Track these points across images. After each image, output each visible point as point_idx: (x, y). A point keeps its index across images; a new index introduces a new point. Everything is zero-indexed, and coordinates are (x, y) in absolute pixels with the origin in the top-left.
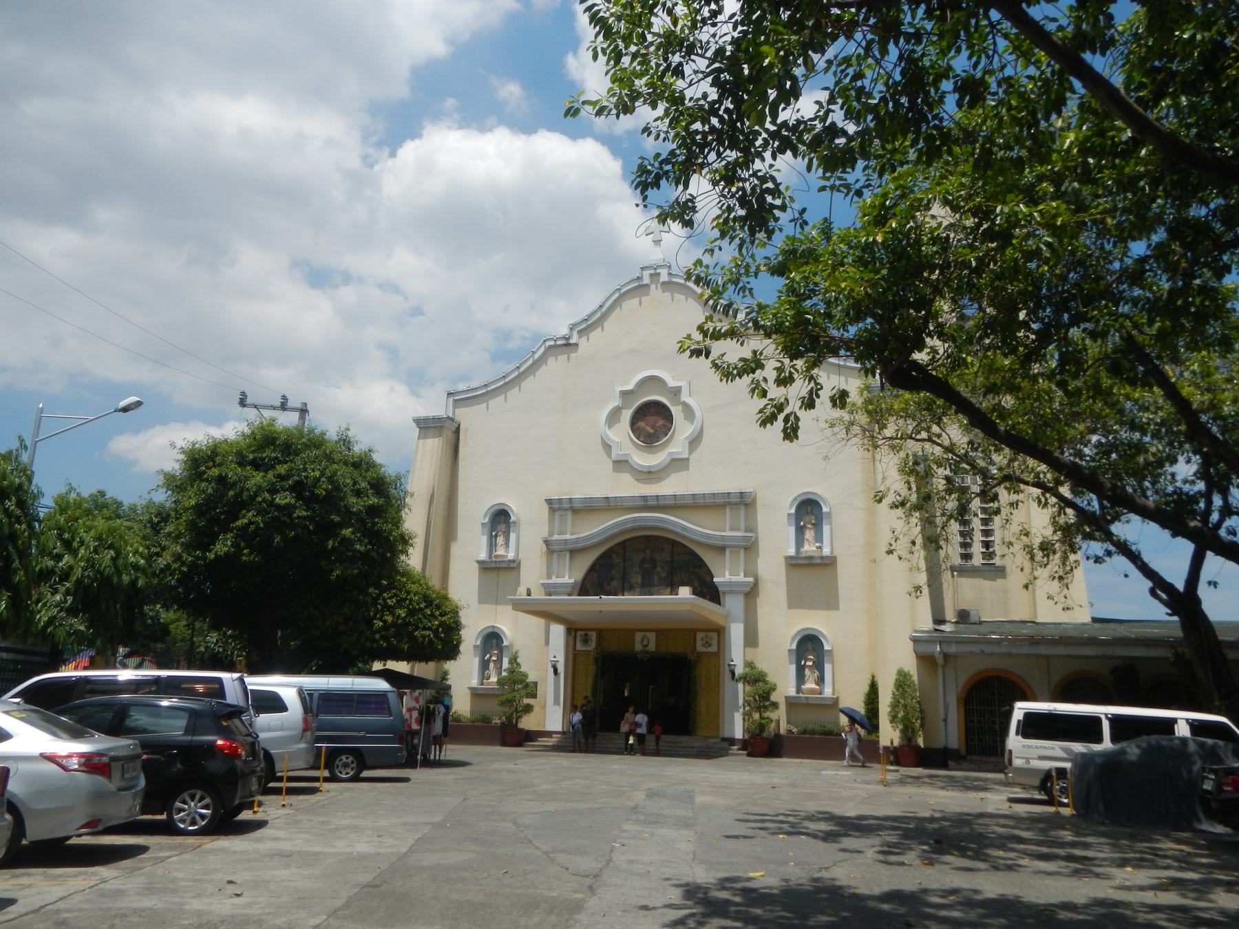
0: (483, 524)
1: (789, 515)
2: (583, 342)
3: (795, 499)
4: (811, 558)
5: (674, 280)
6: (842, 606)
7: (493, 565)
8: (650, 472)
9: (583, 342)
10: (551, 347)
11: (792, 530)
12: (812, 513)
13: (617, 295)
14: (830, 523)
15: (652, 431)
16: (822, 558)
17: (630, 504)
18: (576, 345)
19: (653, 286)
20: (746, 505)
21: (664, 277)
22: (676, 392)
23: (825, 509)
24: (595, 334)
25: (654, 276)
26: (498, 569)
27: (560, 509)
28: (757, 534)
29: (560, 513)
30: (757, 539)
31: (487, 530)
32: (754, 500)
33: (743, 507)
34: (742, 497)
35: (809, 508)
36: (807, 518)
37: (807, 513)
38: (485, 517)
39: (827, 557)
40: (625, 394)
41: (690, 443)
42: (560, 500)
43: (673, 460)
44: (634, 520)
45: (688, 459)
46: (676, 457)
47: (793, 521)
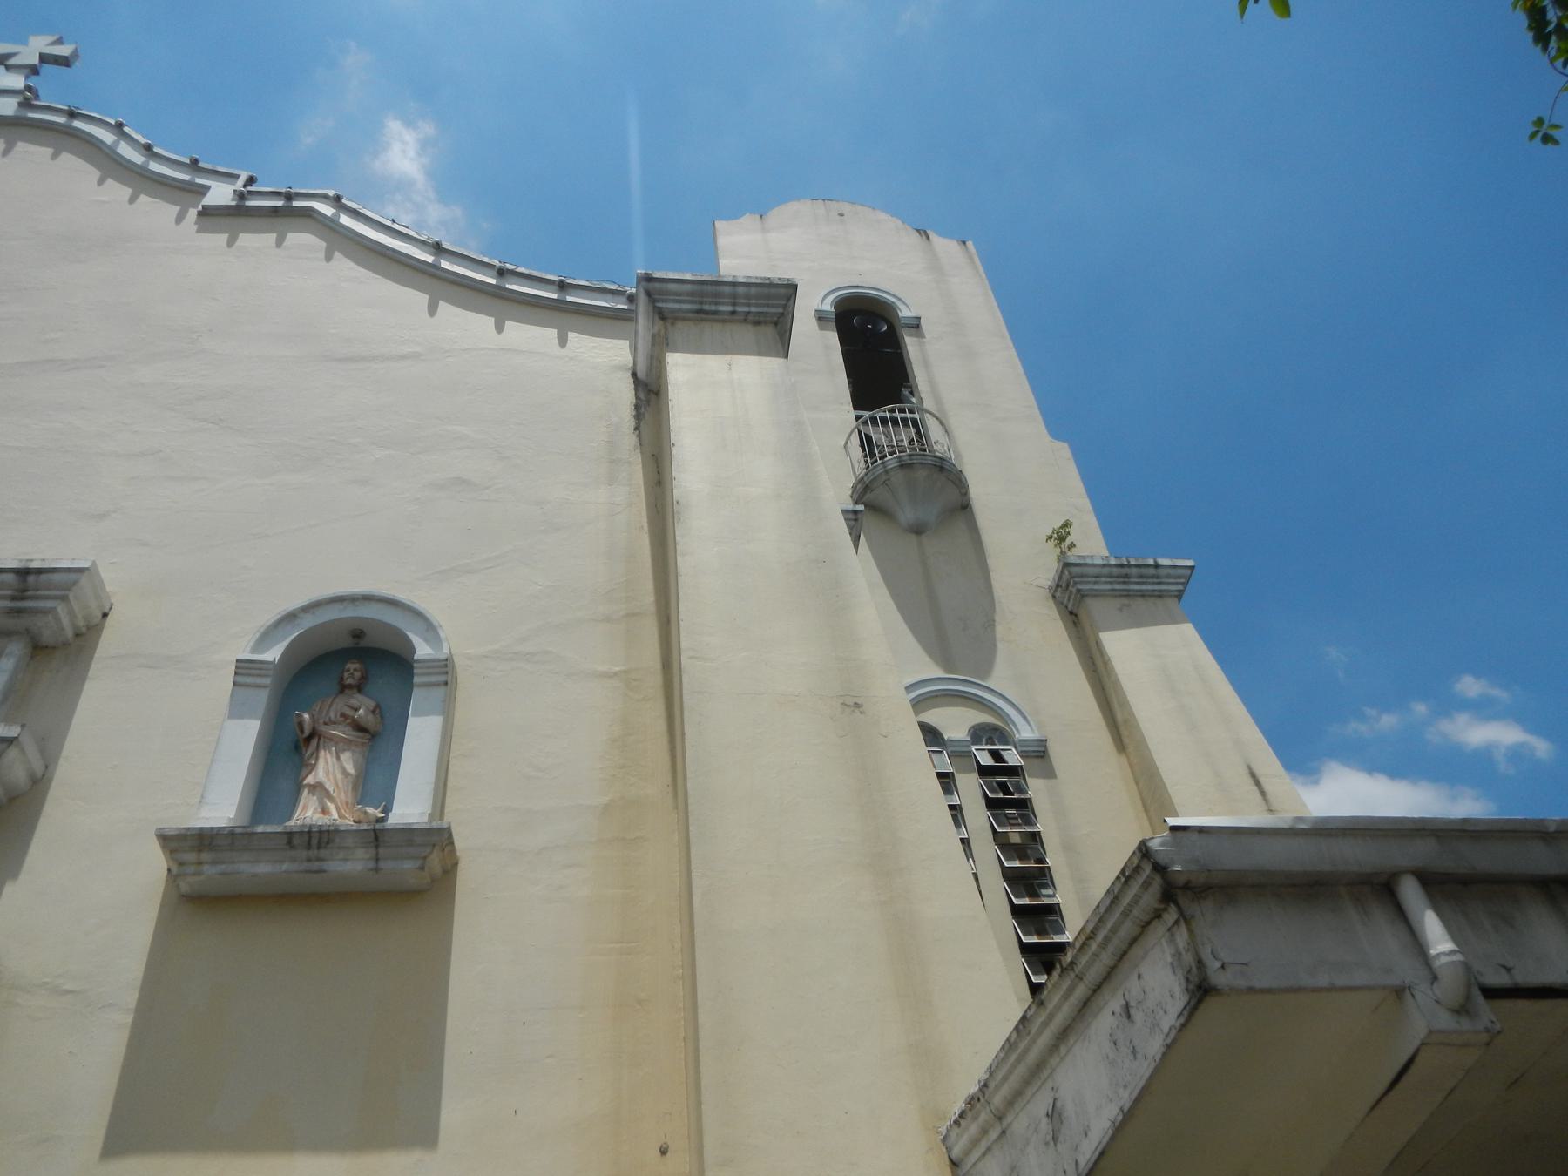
1: (243, 667)
3: (290, 617)
4: (319, 839)
5: (31, 115)
6: (453, 1113)
11: (244, 737)
12: (359, 688)
14: (447, 711)
16: (377, 837)
20: (39, 649)
23: (423, 650)
28: (49, 763)
30: (39, 784)
32: (86, 636)
33: (17, 649)
34: (21, 594)
35: (352, 666)
36: (339, 705)
37: (343, 688)
39: (408, 834)
47: (261, 698)
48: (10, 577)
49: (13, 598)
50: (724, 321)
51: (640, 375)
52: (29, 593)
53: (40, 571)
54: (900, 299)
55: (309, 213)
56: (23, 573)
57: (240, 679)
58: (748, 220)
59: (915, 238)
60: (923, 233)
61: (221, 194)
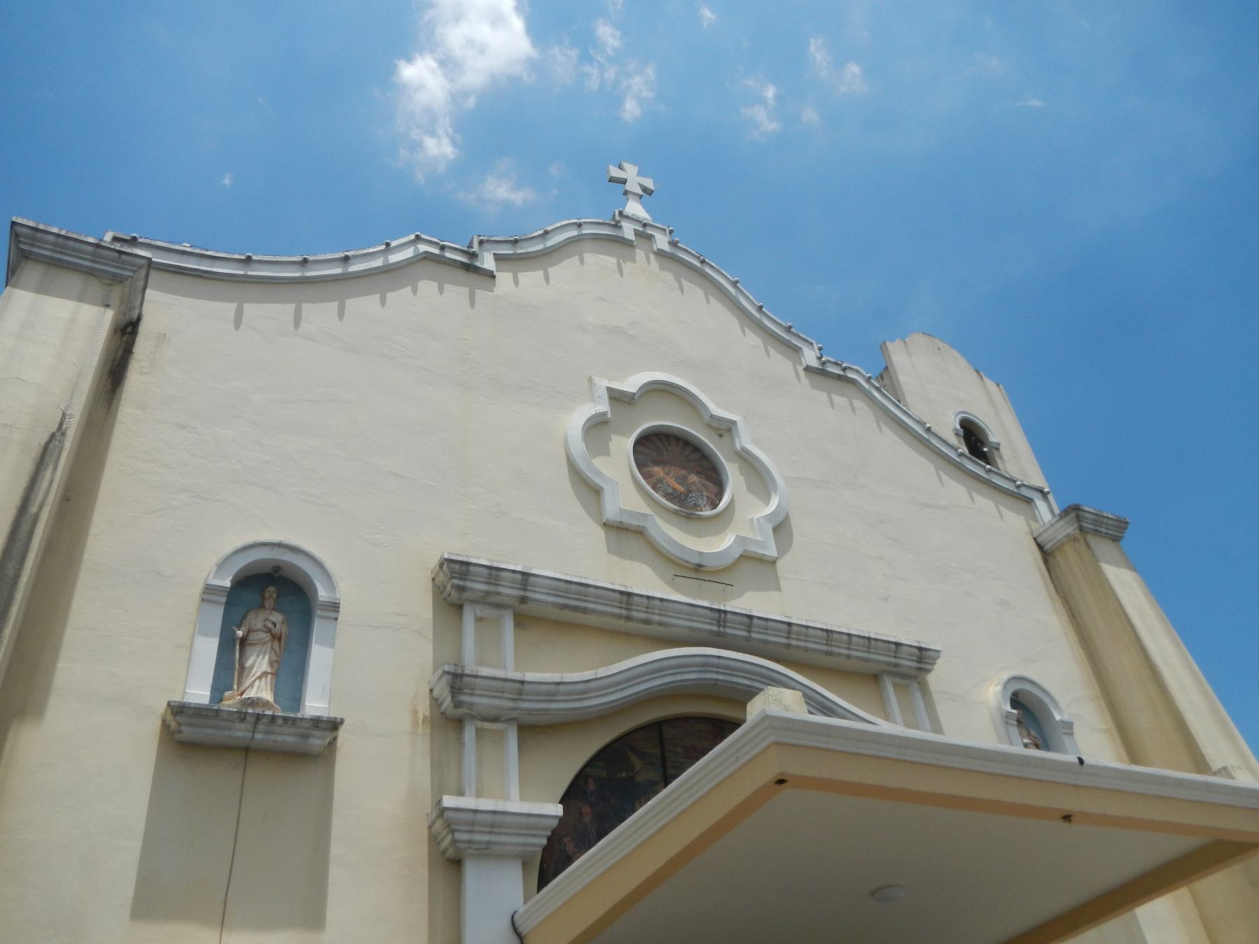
0: (209, 590)
2: (504, 279)
7: (240, 732)
8: (699, 568)
9: (504, 279)
10: (427, 257)
13: (573, 233)
15: (681, 488)
17: (681, 623)
18: (491, 275)
19: (640, 254)
21: (662, 242)
22: (725, 429)
24: (531, 279)
25: (644, 236)
26: (246, 751)
27: (485, 600)
29: (480, 611)
31: (216, 615)
38: (221, 566)
40: (617, 397)
41: (775, 529)
42: (494, 573)
43: (746, 557)
44: (706, 664)
45: (774, 562)
46: (753, 549)
48: (916, 651)
49: (918, 662)
50: (1104, 537)
51: (1039, 540)
52: (923, 660)
53: (926, 649)
54: (987, 427)
55: (853, 382)
56: (920, 649)
57: (1009, 721)
58: (898, 343)
59: (975, 374)
60: (978, 372)
61: (810, 357)
